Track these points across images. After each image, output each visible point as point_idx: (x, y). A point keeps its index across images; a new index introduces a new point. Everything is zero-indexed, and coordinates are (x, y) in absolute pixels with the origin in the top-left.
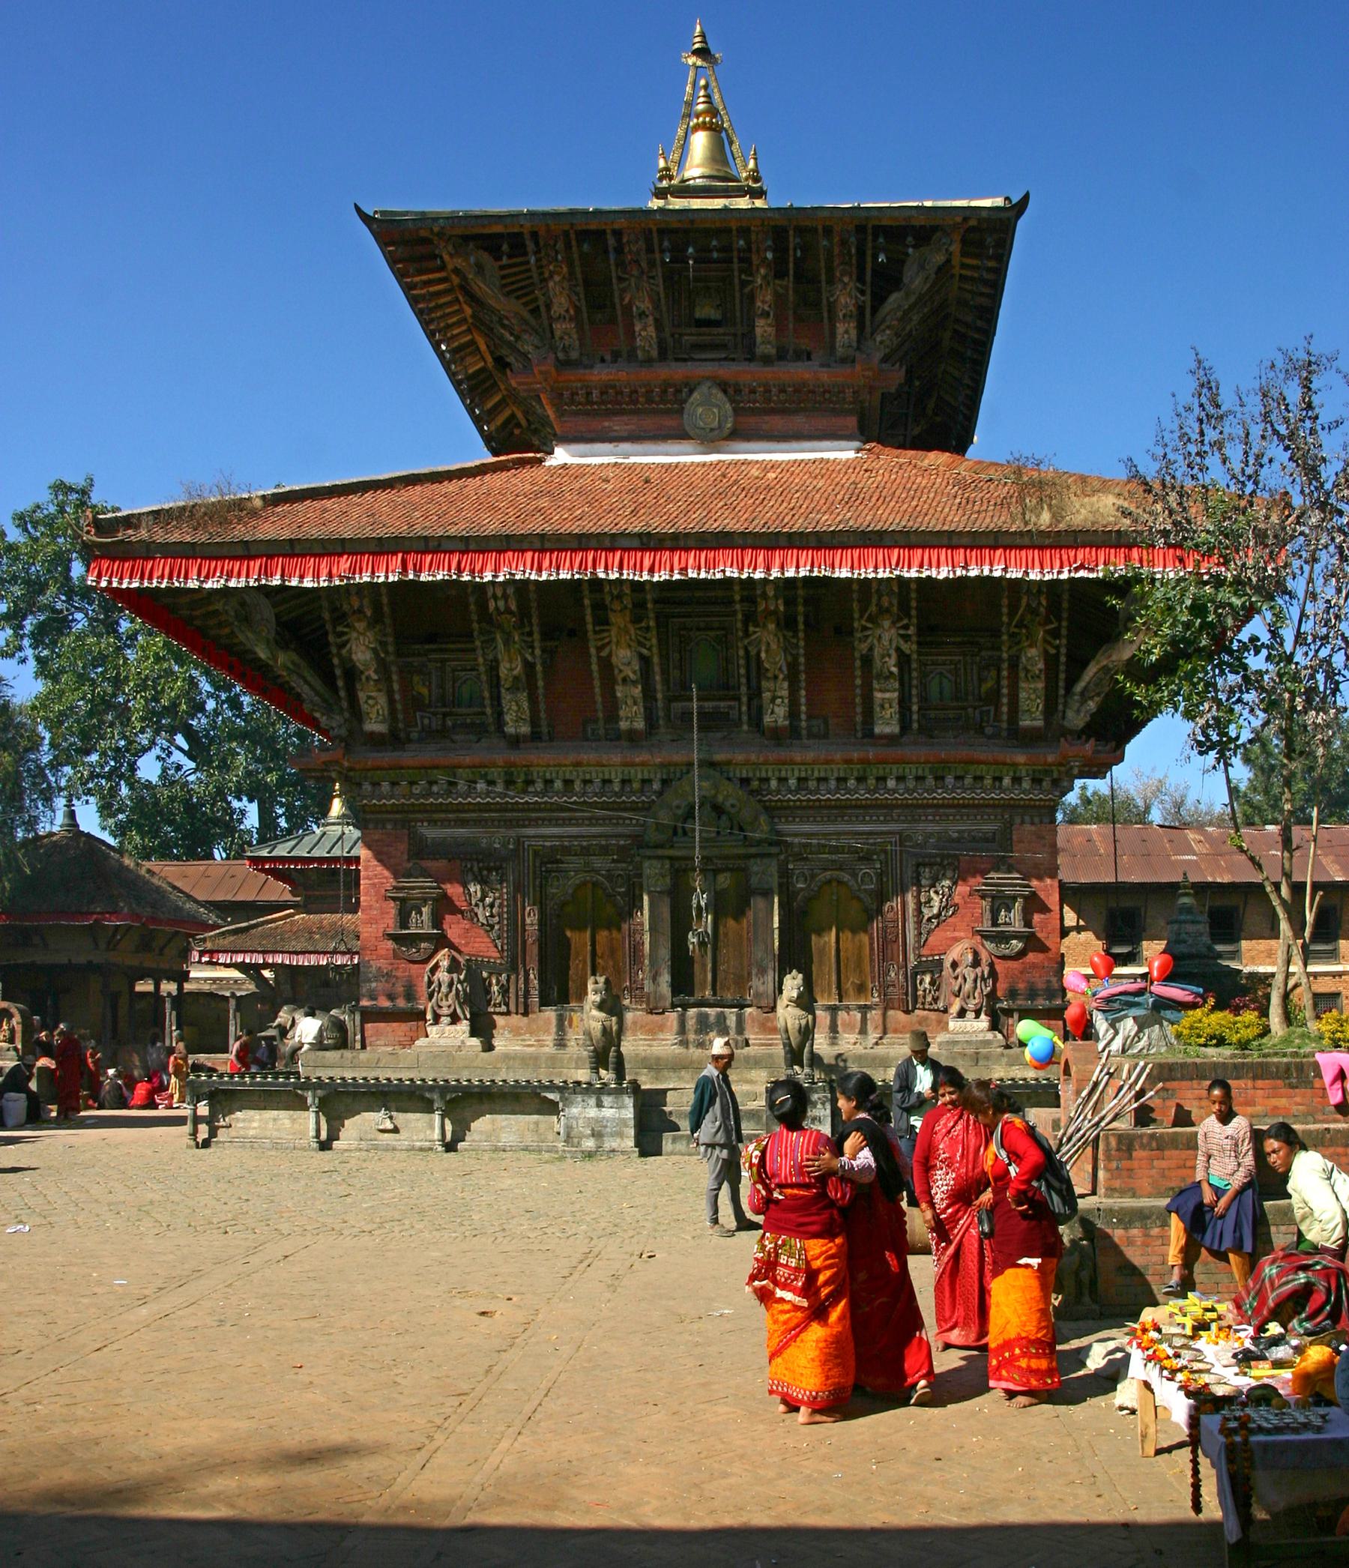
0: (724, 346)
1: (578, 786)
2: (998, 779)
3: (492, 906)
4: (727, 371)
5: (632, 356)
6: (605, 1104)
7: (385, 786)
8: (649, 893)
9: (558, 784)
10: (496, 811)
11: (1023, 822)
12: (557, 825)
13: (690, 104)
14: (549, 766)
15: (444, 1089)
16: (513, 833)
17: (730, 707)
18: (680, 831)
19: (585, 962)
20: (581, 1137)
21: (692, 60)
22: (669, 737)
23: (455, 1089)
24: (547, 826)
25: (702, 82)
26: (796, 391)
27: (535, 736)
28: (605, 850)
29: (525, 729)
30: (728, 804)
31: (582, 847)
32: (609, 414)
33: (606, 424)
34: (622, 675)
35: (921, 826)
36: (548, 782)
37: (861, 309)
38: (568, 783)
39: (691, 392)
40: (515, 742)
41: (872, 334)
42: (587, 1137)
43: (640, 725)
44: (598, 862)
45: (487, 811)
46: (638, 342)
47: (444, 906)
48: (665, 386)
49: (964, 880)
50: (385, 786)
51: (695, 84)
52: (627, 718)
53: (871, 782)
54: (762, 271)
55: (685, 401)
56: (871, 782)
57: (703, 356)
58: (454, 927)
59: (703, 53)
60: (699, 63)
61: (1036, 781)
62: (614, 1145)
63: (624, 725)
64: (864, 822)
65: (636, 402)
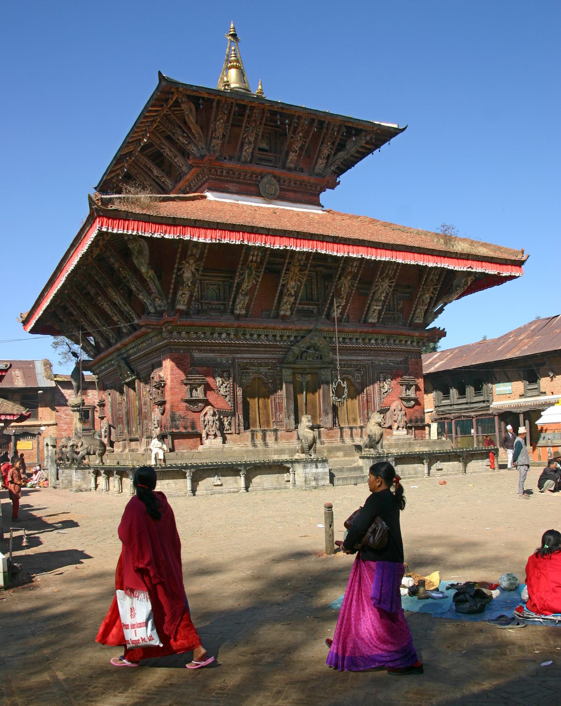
0: (270, 161)
1: (263, 337)
2: (406, 341)
3: (226, 387)
4: (277, 171)
5: (239, 159)
6: (319, 466)
7: (183, 334)
8: (286, 383)
9: (255, 336)
10: (226, 346)
11: (411, 358)
12: (250, 354)
13: (229, 56)
14: (253, 328)
15: (246, 465)
16: (231, 356)
17: (314, 309)
18: (299, 357)
19: (255, 412)
20: (311, 480)
21: (229, 38)
22: (296, 319)
23: (250, 464)
24: (247, 354)
25: (233, 48)
26: (301, 184)
27: (246, 316)
28: (267, 364)
29: (244, 312)
30: (321, 347)
31: (258, 363)
32: (228, 182)
33: (227, 186)
34: (289, 292)
35: (379, 358)
36: (252, 335)
37: (328, 158)
38: (259, 335)
39: (262, 178)
40: (238, 317)
41: (330, 166)
42: (312, 481)
43: (288, 313)
44: (263, 370)
45: (224, 346)
46: (244, 153)
47: (208, 388)
48: (253, 173)
49: (395, 379)
50: (183, 334)
51: (230, 48)
52: (284, 310)
53: (367, 340)
54: (301, 134)
55: (260, 181)
56: (367, 340)
57: (265, 164)
58: (211, 397)
59: (234, 36)
60: (232, 40)
61: (418, 343)
62: (323, 483)
63: (282, 313)
64: (362, 356)
65: (239, 178)
